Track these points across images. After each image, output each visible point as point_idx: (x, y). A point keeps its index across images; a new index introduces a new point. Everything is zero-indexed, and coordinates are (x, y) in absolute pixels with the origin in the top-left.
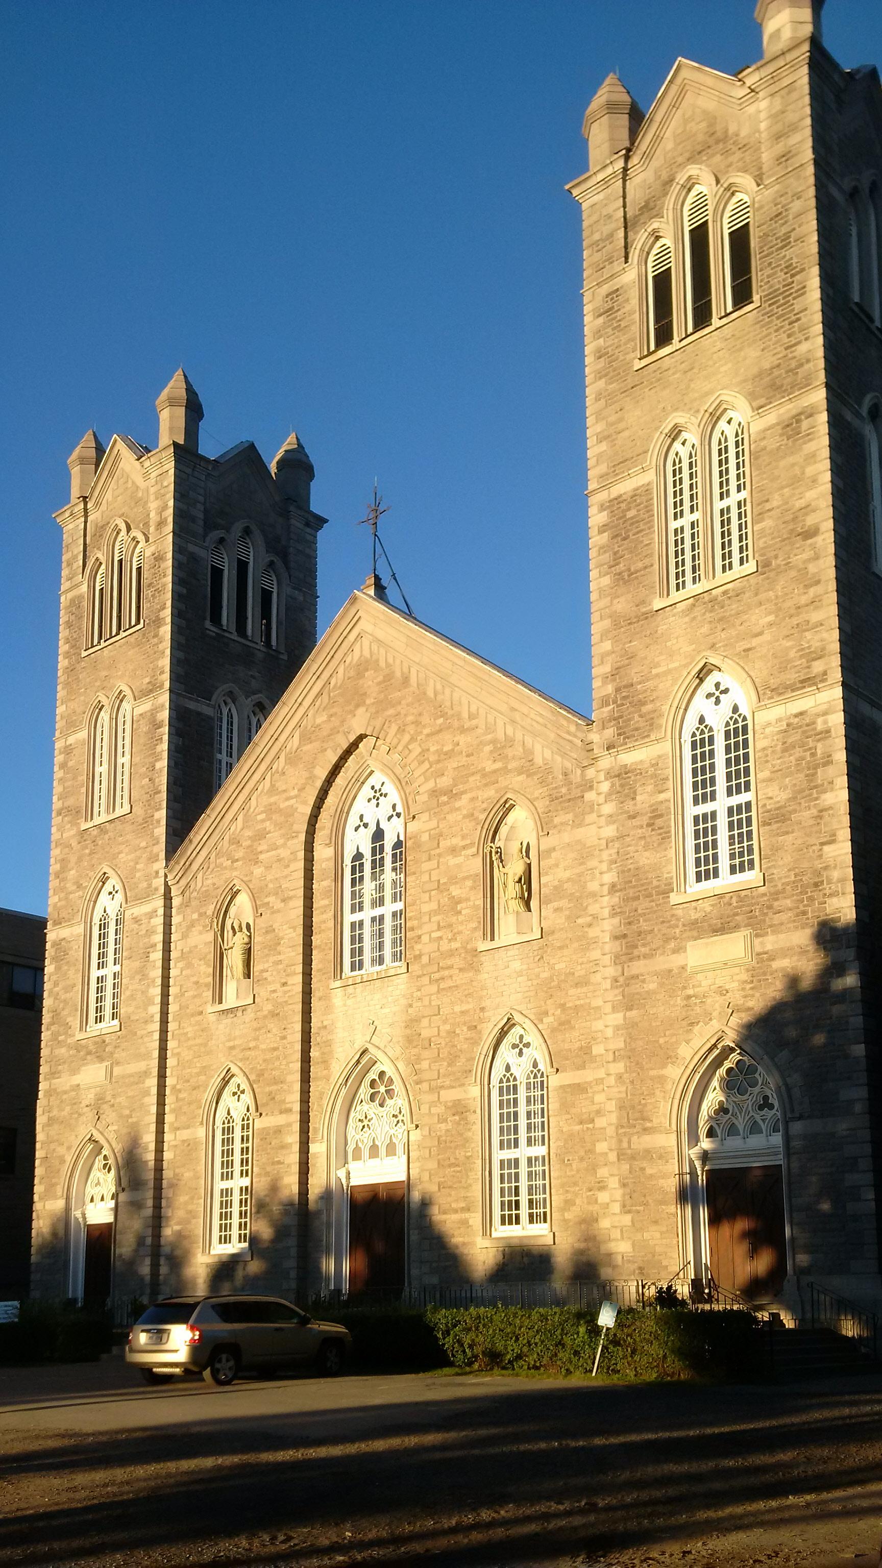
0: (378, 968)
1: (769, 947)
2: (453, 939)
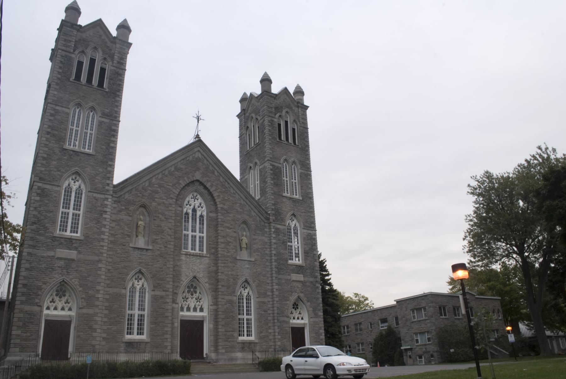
0: (193, 251)
2: (228, 252)
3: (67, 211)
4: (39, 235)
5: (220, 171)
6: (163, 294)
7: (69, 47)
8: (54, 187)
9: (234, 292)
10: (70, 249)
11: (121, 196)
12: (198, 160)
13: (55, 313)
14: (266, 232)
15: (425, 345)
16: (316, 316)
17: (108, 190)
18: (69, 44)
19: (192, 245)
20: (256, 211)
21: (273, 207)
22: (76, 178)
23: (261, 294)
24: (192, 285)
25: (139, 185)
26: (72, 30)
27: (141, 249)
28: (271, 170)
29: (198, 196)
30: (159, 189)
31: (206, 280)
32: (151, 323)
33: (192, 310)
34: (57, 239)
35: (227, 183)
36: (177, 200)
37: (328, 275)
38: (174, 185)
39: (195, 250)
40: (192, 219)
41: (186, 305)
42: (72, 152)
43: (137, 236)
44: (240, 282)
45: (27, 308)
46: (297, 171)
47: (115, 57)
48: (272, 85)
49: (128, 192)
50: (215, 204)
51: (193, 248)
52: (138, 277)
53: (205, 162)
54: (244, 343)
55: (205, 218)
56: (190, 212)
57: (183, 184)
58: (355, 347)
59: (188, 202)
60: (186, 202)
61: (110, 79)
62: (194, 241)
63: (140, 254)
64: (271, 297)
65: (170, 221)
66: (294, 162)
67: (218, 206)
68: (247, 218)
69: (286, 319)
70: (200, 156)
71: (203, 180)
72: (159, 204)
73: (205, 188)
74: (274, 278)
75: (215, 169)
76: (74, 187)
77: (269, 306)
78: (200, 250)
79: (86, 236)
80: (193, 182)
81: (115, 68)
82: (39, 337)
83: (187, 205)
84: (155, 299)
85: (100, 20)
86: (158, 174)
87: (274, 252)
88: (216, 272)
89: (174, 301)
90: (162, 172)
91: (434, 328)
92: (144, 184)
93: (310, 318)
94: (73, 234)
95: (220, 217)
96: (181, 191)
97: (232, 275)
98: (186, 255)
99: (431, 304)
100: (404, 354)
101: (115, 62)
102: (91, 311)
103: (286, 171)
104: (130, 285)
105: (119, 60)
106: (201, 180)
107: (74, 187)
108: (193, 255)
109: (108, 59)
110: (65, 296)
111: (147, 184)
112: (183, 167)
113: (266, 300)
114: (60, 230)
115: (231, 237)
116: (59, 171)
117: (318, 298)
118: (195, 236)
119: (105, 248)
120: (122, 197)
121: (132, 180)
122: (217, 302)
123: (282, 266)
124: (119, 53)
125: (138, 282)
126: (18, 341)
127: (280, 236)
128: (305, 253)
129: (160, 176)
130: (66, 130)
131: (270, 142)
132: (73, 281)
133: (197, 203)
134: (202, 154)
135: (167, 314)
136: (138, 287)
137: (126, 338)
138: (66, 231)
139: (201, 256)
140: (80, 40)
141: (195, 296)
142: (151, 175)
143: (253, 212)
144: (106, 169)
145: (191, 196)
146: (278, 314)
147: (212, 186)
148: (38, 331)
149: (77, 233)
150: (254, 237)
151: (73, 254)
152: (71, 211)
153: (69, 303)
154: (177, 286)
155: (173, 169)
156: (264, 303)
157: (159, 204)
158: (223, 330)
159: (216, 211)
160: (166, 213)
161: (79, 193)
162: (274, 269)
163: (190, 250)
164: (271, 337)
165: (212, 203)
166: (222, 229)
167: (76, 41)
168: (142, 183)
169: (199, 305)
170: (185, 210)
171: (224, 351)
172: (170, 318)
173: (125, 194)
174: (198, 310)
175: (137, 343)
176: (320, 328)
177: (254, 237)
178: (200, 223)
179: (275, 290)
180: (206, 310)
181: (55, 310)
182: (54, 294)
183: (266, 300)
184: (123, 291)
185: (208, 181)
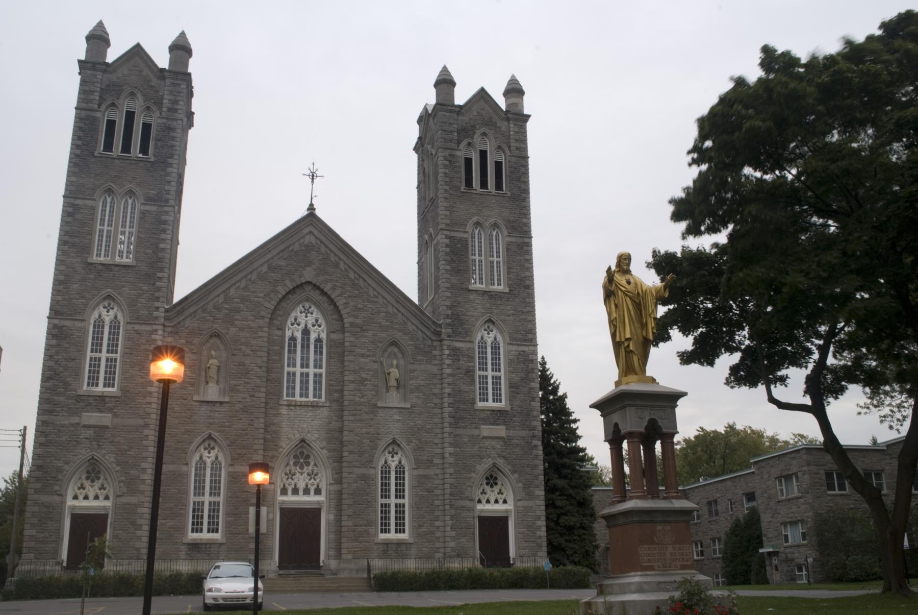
0: (304, 399)
2: (363, 397)
3: (97, 355)
5: (349, 262)
7: (90, 101)
8: (76, 322)
9: (371, 461)
10: (102, 412)
11: (179, 323)
13: (85, 503)
14: (435, 356)
15: (798, 546)
16: (530, 496)
17: (156, 318)
18: (91, 97)
19: (301, 388)
20: (416, 322)
21: (449, 312)
22: (109, 304)
23: (418, 464)
24: (302, 453)
25: (207, 303)
26: (95, 73)
27: (211, 402)
28: (447, 246)
30: (241, 306)
31: (324, 444)
32: (227, 514)
33: (301, 492)
35: (361, 281)
36: (271, 319)
37: (575, 421)
39: (307, 396)
40: (302, 346)
42: (100, 267)
43: (207, 383)
45: (44, 498)
46: (501, 239)
47: (165, 101)
48: (456, 89)
49: (190, 315)
50: (341, 319)
51: (304, 394)
52: (209, 445)
53: (323, 249)
54: (387, 544)
55: (324, 342)
56: (299, 335)
57: (282, 291)
58: (710, 546)
59: (296, 320)
60: (291, 319)
61: (158, 140)
63: (211, 411)
64: (440, 466)
65: (259, 354)
67: (345, 321)
68: (398, 335)
69: (468, 503)
71: (317, 281)
72: (241, 329)
73: (323, 293)
74: (446, 435)
75: (340, 259)
76: (108, 318)
77: (436, 482)
78: (315, 396)
79: (124, 390)
80: (301, 286)
81: (164, 120)
82: (60, 538)
83: (292, 324)
85: (138, 46)
86: (240, 280)
87: (447, 391)
88: (341, 431)
90: (246, 276)
91: (810, 514)
92: (215, 300)
93: (517, 500)
95: (349, 338)
96: (278, 303)
97: (368, 433)
98: (288, 405)
99: (805, 468)
100: (767, 562)
101: (164, 109)
102: (133, 500)
103: (480, 242)
105: (170, 106)
106: (314, 281)
107: (108, 318)
108: (300, 406)
109: (154, 108)
110: (98, 478)
111: (221, 299)
112: (283, 263)
113: (431, 472)
114: (88, 385)
115: (369, 370)
116: (83, 297)
117: (536, 466)
120: (182, 324)
121: (196, 296)
122: (341, 478)
123: (464, 411)
124: (171, 93)
125: (209, 453)
126: (32, 544)
127: (461, 362)
128: (510, 387)
130: (91, 233)
131: (447, 195)
132: (107, 457)
133: (311, 319)
134: (316, 237)
136: (209, 461)
138: (97, 385)
139: (314, 406)
140: (108, 86)
141: (307, 470)
142: (228, 285)
143: (409, 324)
144: (154, 284)
146: (451, 495)
147: (334, 288)
148: (59, 531)
149: (113, 386)
150: (411, 367)
151: (105, 419)
152: (104, 355)
153: (105, 489)
154: (273, 457)
155: (264, 269)
156: (426, 477)
157: (241, 329)
158: (350, 523)
159: (343, 330)
160: (253, 342)
161: (115, 325)
162: (447, 420)
163: (297, 398)
164: (438, 534)
165: (336, 316)
166: (352, 358)
167: (102, 89)
168: (213, 300)
169: (312, 485)
170: (288, 334)
171: (350, 557)
173: (184, 319)
174: (312, 492)
175: (206, 544)
176: (538, 518)
177: (411, 367)
178: (316, 352)
179: (447, 455)
180: (323, 492)
181: (82, 499)
183: (431, 472)
184: (184, 468)
185: (327, 281)
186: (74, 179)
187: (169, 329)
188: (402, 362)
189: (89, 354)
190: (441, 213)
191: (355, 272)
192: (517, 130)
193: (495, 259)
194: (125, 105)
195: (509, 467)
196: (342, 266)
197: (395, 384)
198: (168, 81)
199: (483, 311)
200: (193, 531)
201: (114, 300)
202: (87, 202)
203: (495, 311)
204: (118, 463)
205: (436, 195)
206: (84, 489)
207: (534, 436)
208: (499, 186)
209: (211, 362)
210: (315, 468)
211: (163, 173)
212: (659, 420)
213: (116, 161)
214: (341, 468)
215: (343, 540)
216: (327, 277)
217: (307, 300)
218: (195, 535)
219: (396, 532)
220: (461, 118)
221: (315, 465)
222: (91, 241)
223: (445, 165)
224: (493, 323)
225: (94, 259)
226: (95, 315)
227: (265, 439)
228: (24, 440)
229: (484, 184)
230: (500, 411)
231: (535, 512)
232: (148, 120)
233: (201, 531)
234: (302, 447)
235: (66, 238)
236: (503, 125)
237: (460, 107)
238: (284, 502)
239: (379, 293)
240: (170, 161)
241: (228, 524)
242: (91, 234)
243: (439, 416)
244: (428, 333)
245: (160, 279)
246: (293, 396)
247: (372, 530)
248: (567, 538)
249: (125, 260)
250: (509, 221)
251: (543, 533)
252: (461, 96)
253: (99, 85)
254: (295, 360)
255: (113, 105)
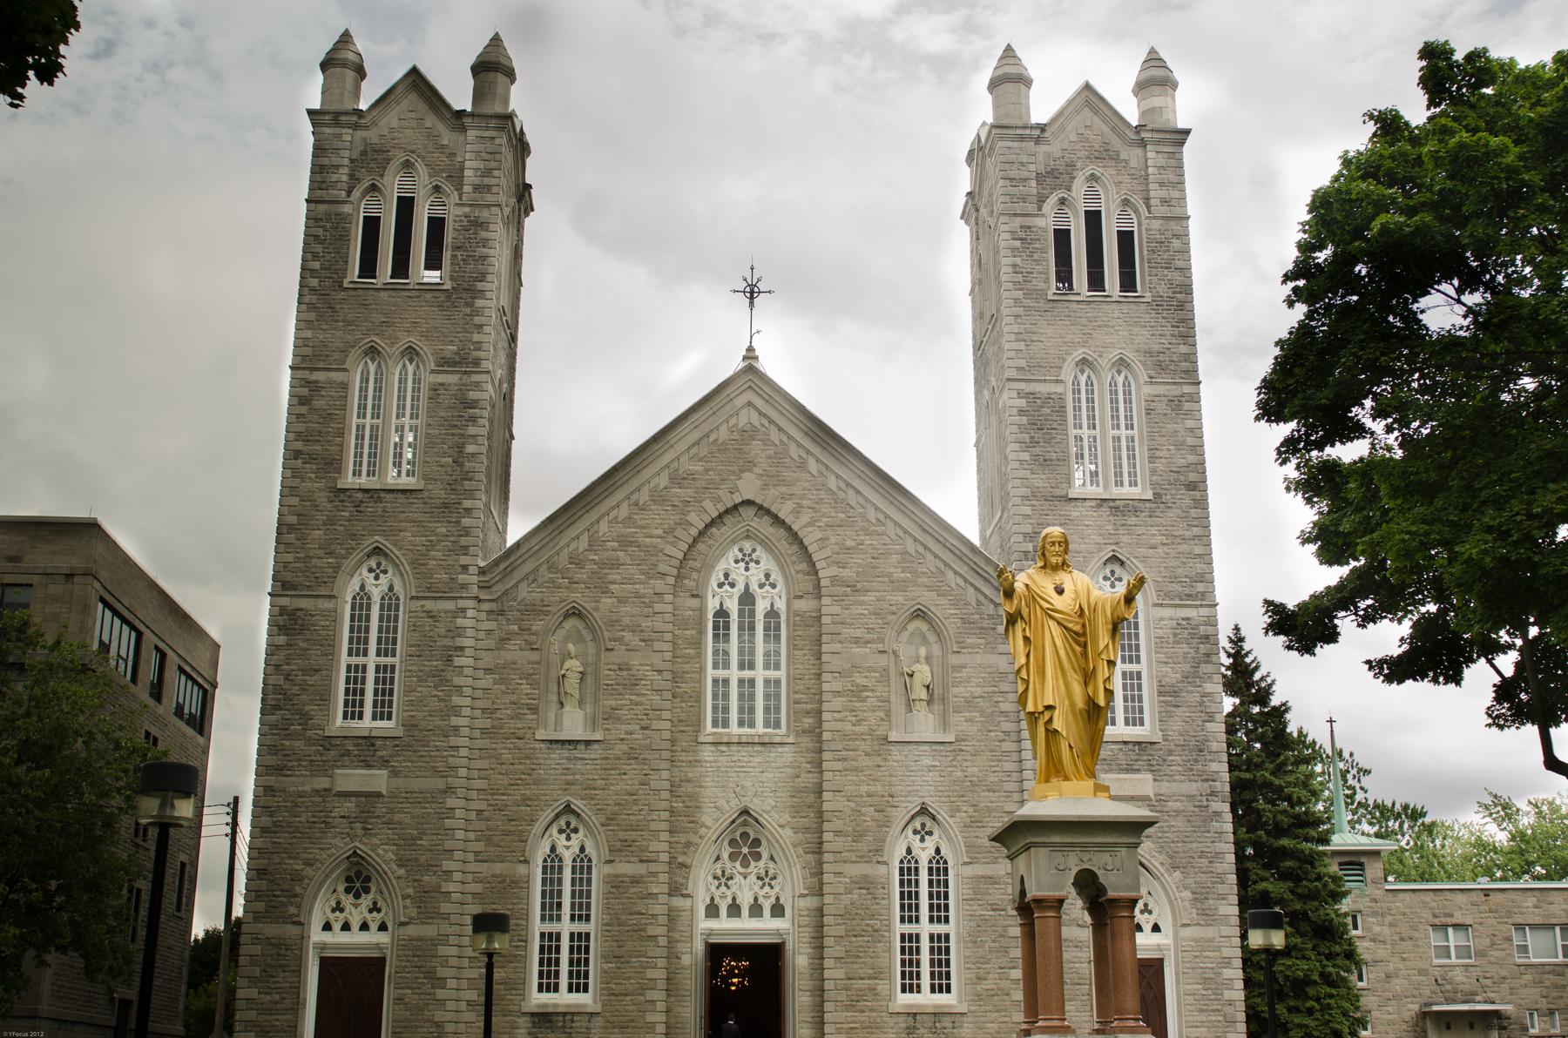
0: (746, 730)
1: (1163, 791)
2: (859, 722)
3: (360, 660)
4: (289, 736)
6: (641, 869)
8: (320, 601)
9: (879, 850)
10: (369, 767)
11: (506, 593)
12: (748, 434)
16: (1208, 916)
17: (464, 586)
18: (334, 178)
20: (963, 570)
22: (379, 565)
24: (745, 835)
26: (338, 130)
28: (1021, 412)
29: (760, 553)
31: (787, 817)
32: (605, 957)
33: (745, 911)
34: (334, 742)
35: (851, 493)
36: (679, 577)
38: (669, 531)
39: (752, 725)
40: (741, 628)
41: (723, 897)
42: (360, 495)
44: (900, 816)
45: (270, 930)
47: (467, 173)
49: (526, 577)
51: (747, 720)
52: (568, 824)
53: (775, 435)
55: (783, 618)
56: (733, 607)
59: (726, 576)
62: (747, 696)
63: (568, 759)
65: (657, 646)
66: (1122, 364)
67: (821, 573)
68: (928, 599)
70: (755, 419)
73: (778, 521)
75: (808, 452)
76: (376, 592)
78: (767, 724)
79: (410, 726)
81: (467, 209)
83: (721, 585)
84: (615, 885)
88: (819, 792)
89: (676, 890)
92: (573, 546)
94: (379, 724)
95: (829, 607)
101: (467, 189)
102: (429, 931)
104: (545, 848)
105: (477, 181)
107: (376, 592)
109: (447, 187)
112: (698, 468)
116: (331, 554)
118: (752, 682)
119: (464, 752)
122: (821, 884)
125: (568, 838)
126: (252, 1015)
128: (1160, 693)
129: (624, 512)
131: (1020, 310)
133: (756, 574)
134: (760, 413)
135: (651, 931)
137: (534, 1002)
138: (361, 718)
140: (364, 153)
141: (756, 867)
143: (950, 574)
144: (458, 522)
145: (735, 552)
147: (797, 512)
148: (297, 989)
149: (389, 718)
150: (954, 660)
151: (379, 779)
153: (379, 911)
154: (688, 844)
155: (663, 480)
158: (840, 974)
159: (817, 592)
160: (645, 624)
161: (390, 604)
166: (837, 647)
167: (352, 161)
170: (712, 605)
172: (663, 941)
173: (516, 586)
175: (564, 1014)
176: (1227, 962)
177: (954, 660)
180: (788, 912)
182: (341, 888)
184: (522, 869)
185: (784, 498)
186: (308, 334)
187: (485, 606)
188: (936, 650)
189: (344, 659)
190: (1007, 346)
191: (838, 476)
192: (1161, 161)
193: (1123, 432)
194: (394, 186)
195: (1162, 857)
196: (813, 466)
197: (924, 694)
198: (472, 134)
199: (1099, 539)
200: (540, 990)
201: (386, 555)
202: (335, 376)
203: (1124, 539)
204: (401, 862)
205: (998, 311)
206: (342, 911)
207: (1213, 793)
208: (1128, 282)
209: (567, 665)
210: (772, 865)
211: (468, 311)
212: (1100, 873)
213: (382, 294)
214: (820, 864)
215: (828, 1006)
216: (783, 489)
217: (748, 537)
218: (547, 998)
219: (933, 990)
220: (1043, 148)
221: (772, 858)
222: (342, 447)
223: (1013, 249)
224: (1122, 563)
225: (349, 480)
226: (354, 586)
227: (672, 811)
228: (234, 825)
229: (1096, 281)
230: (1139, 743)
231: (1219, 949)
232: (438, 213)
233: (556, 990)
234: (745, 824)
235: (299, 445)
236: (1133, 156)
237: (1042, 128)
238: (711, 933)
239: (887, 516)
240: (480, 286)
241: (607, 977)
242: (342, 435)
243: (1015, 757)
244: (988, 591)
245: (468, 511)
246: (726, 724)
247: (882, 986)
248: (1292, 1003)
249: (406, 481)
250: (1150, 353)
251: (1237, 993)
252: (1042, 106)
253: (347, 153)
254: (726, 653)
255: (374, 188)
